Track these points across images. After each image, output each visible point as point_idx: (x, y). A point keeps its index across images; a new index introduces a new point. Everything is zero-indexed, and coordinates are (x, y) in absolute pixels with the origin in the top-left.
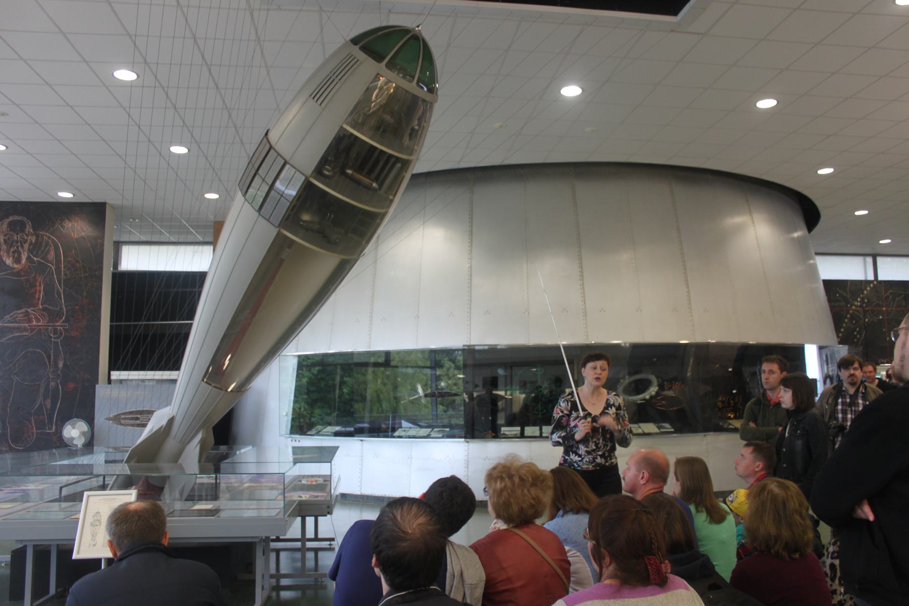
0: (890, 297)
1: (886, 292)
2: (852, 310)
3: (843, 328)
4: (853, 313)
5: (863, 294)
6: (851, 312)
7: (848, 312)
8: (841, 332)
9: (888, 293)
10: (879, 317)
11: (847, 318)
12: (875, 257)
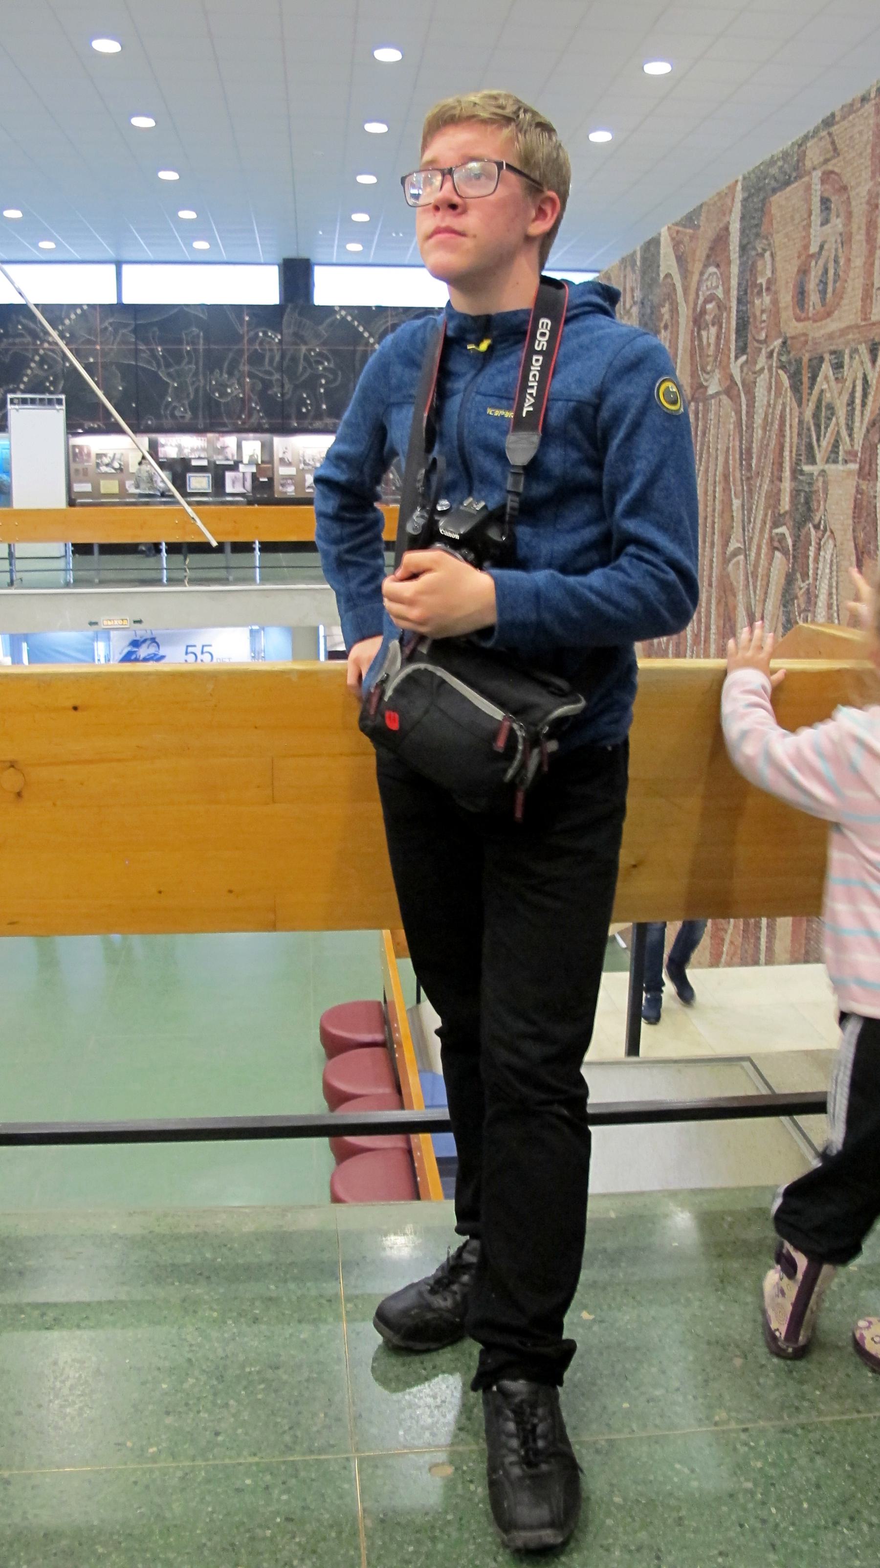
0: (110, 329)
1: (102, 321)
2: (44, 349)
3: (27, 375)
4: (45, 354)
5: (63, 324)
6: (41, 352)
7: (36, 352)
8: (24, 383)
9: (106, 324)
10: (88, 359)
11: (35, 362)
12: (119, 264)
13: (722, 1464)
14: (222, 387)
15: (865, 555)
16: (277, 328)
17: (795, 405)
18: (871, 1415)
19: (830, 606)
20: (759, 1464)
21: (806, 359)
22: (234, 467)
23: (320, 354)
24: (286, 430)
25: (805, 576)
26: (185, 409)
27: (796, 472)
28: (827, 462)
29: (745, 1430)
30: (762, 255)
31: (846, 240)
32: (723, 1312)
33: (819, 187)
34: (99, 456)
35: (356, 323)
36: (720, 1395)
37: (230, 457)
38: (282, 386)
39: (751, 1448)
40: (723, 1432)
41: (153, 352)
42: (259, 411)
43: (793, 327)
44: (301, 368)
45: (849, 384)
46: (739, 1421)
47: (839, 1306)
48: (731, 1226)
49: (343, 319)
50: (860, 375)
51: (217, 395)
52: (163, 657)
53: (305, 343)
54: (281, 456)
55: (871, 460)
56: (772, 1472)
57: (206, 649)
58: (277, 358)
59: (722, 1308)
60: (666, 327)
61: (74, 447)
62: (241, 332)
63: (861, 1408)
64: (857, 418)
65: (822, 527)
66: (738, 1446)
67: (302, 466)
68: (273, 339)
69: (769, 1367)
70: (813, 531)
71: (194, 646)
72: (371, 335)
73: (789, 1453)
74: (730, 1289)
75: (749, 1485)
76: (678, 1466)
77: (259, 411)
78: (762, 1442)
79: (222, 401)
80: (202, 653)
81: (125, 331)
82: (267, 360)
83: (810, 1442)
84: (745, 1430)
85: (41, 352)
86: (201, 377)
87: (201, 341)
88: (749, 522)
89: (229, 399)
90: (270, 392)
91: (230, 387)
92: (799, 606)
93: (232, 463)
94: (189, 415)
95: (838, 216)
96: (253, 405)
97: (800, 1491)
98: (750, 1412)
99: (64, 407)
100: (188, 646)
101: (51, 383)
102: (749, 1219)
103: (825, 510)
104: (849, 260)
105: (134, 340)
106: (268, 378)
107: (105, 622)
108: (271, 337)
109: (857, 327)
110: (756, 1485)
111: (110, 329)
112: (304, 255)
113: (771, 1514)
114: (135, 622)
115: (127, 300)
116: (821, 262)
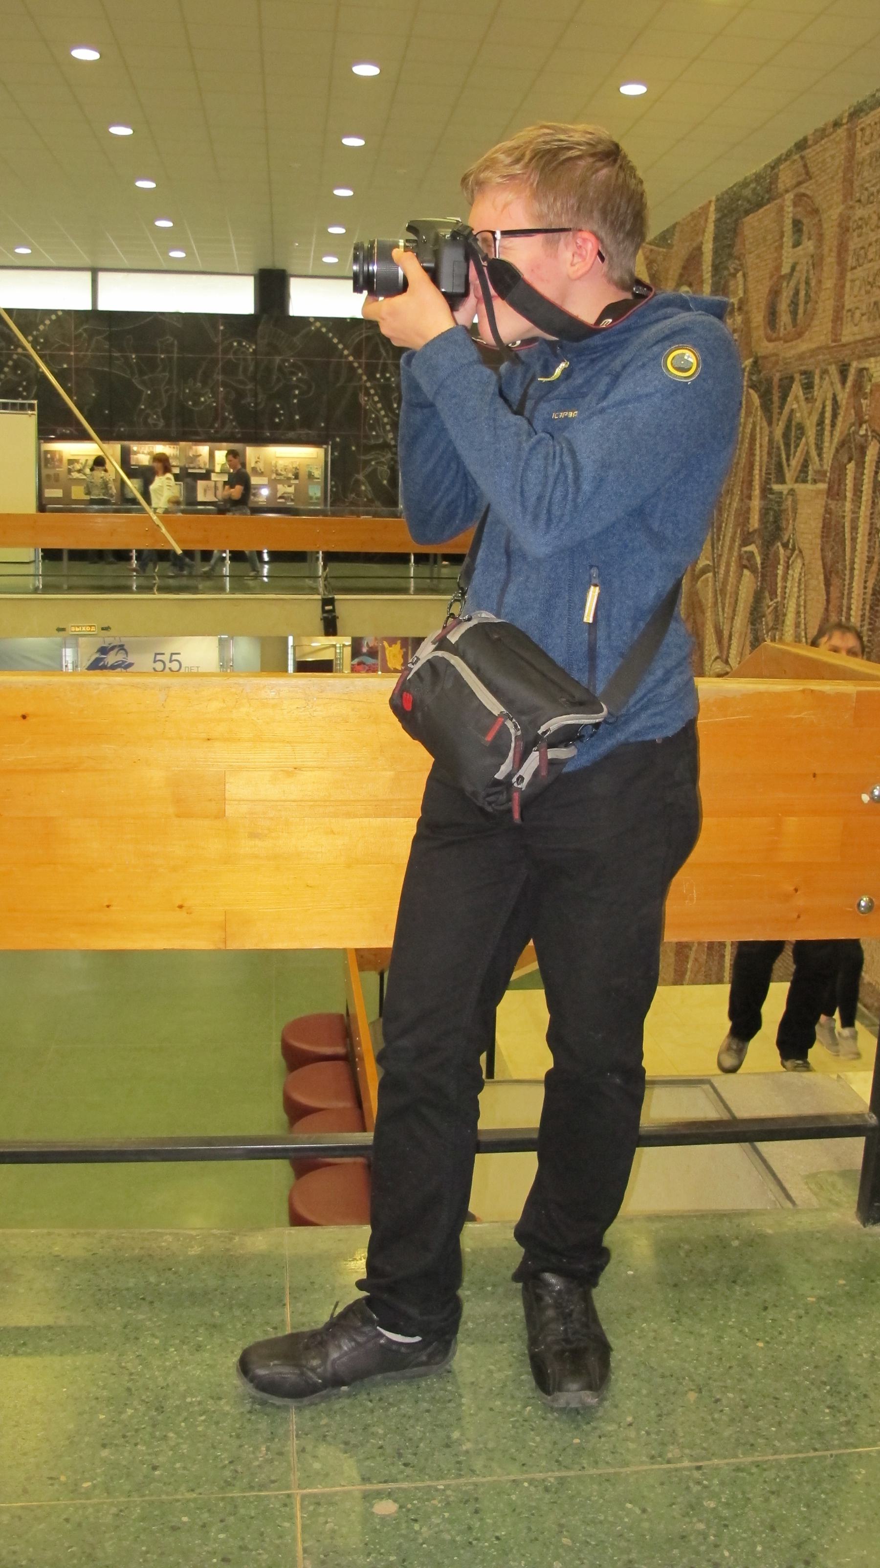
0: (85, 335)
1: (76, 328)
5: (38, 330)
6: (15, 357)
7: (10, 357)
11: (8, 366)
12: (95, 272)
13: (674, 1504)
14: (195, 396)
15: (833, 575)
16: (252, 338)
17: (765, 424)
18: (828, 1453)
19: (797, 625)
20: (712, 1505)
22: (206, 476)
23: (293, 365)
24: (260, 441)
25: (773, 594)
26: (158, 416)
27: (766, 491)
28: (796, 481)
29: (699, 1468)
30: (734, 275)
31: (817, 262)
32: (677, 1344)
33: (791, 209)
34: (71, 462)
35: (330, 335)
36: (674, 1432)
37: (202, 466)
38: (256, 396)
39: (706, 1487)
40: (676, 1470)
41: (127, 359)
42: (232, 421)
43: (765, 347)
44: (275, 377)
45: (818, 404)
46: (692, 1458)
47: (796, 1339)
48: (688, 1254)
49: (318, 330)
50: (830, 395)
51: (190, 403)
52: (131, 665)
53: (280, 354)
54: (253, 465)
55: (840, 480)
56: (725, 1513)
57: (174, 657)
58: (251, 368)
59: (677, 1340)
61: (47, 452)
62: (215, 341)
63: (818, 1446)
65: (790, 546)
66: (691, 1484)
67: (274, 476)
68: (248, 349)
69: (724, 1402)
70: (781, 550)
71: (163, 654)
72: (345, 347)
73: (744, 1493)
74: (685, 1320)
75: (701, 1526)
76: (629, 1506)
77: (232, 421)
78: (716, 1482)
79: (196, 409)
80: (171, 661)
81: (99, 338)
82: (241, 368)
83: (765, 1482)
84: (699, 1468)
85: (15, 357)
86: (175, 386)
87: (176, 350)
88: (719, 539)
89: (203, 407)
90: (243, 402)
91: (203, 395)
92: (767, 624)
93: (204, 471)
94: (162, 423)
95: (809, 239)
96: (227, 414)
97: (754, 1533)
98: (704, 1449)
99: (36, 412)
100: (156, 654)
101: (25, 388)
102: (706, 1247)
103: (794, 529)
104: (820, 282)
105: (107, 347)
106: (242, 387)
107: (73, 629)
108: (245, 346)
109: (828, 347)
110: (709, 1527)
111: (85, 335)
112: (279, 266)
113: (723, 1556)
114: (103, 629)
115: (102, 307)
116: (793, 284)
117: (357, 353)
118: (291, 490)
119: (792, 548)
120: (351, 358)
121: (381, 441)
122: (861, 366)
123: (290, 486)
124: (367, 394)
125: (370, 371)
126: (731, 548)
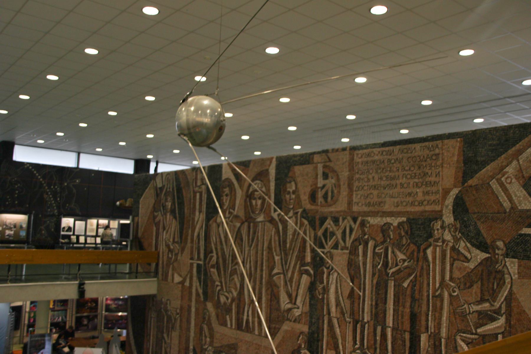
19: (337, 292)
21: (317, 217)
28: (332, 248)
30: (290, 182)
31: (338, 185)
33: (321, 168)
35: (33, 170)
43: (308, 206)
45: (342, 227)
49: (28, 167)
60: (227, 195)
64: (348, 239)
65: (330, 268)
67: (5, 227)
70: (325, 270)
72: (39, 175)
88: (286, 264)
92: (319, 292)
95: (332, 178)
104: (339, 192)
109: (345, 211)
116: (324, 191)
117: (44, 177)
118: (12, 232)
119: (331, 270)
120: (41, 180)
121: (52, 213)
122: (363, 218)
123: (12, 231)
124: (47, 194)
125: (49, 185)
126: (295, 267)
